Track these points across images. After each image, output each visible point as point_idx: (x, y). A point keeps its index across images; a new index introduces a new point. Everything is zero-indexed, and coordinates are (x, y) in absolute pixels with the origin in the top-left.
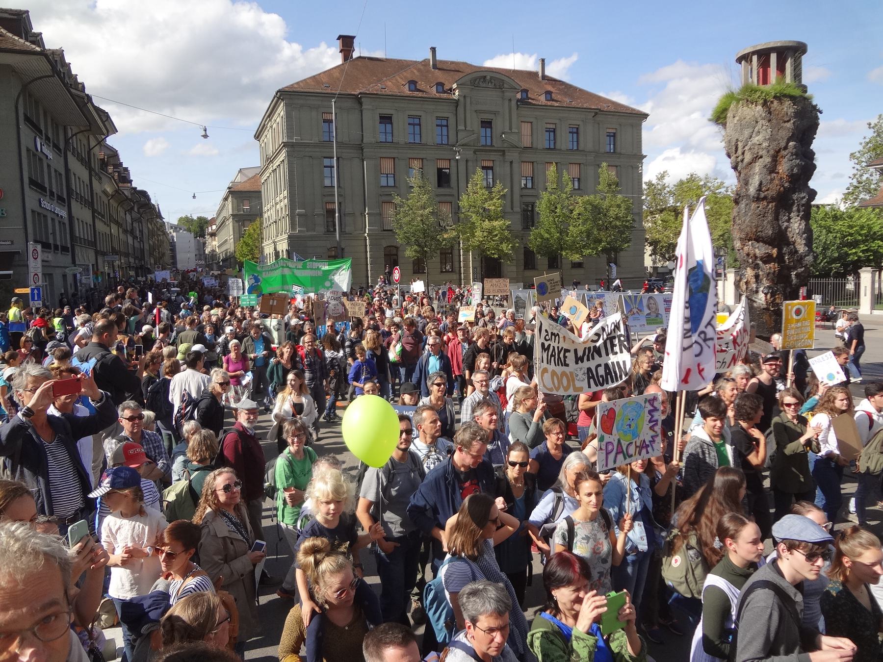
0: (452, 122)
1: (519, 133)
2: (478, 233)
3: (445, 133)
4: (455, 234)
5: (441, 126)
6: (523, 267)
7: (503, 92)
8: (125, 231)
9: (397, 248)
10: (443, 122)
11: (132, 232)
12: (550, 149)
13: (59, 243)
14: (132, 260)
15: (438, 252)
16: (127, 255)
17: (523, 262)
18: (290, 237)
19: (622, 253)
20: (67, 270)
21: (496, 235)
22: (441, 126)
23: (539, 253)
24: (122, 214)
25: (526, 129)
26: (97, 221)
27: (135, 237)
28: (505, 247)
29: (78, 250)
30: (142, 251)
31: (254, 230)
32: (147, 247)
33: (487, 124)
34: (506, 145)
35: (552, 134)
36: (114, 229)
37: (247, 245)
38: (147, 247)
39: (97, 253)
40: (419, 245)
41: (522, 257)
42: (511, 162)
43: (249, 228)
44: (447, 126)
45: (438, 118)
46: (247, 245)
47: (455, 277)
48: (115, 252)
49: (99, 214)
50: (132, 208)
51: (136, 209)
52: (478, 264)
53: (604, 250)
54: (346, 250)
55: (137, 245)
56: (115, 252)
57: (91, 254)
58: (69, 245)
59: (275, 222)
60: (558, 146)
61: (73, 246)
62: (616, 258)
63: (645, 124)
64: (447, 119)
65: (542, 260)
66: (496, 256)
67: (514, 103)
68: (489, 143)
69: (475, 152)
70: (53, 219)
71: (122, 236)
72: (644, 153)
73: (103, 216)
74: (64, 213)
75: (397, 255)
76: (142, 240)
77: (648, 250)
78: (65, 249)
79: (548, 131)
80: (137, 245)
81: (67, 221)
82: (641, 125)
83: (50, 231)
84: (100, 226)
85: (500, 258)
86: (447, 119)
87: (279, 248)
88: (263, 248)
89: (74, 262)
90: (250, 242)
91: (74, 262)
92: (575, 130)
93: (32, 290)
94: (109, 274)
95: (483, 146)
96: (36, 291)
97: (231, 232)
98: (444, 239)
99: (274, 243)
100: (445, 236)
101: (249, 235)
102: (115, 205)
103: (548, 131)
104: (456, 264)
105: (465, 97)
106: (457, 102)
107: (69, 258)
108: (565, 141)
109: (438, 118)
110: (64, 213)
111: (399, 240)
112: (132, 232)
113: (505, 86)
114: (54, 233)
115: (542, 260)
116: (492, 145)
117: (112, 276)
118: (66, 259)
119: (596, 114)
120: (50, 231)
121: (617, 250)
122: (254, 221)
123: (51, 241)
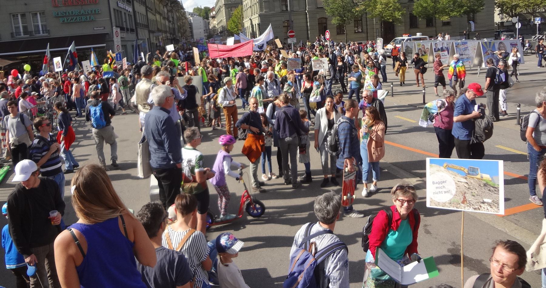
2: (379, 6)
4: (364, 7)
6: (409, 27)
8: (164, 18)
9: (326, 19)
11: (168, 19)
13: (129, 27)
14: (168, 35)
15: (353, 20)
16: (166, 32)
17: (408, 23)
18: (260, 16)
19: (478, 14)
21: (391, 7)
23: (420, 17)
24: (162, 8)
26: (148, 13)
27: (169, 22)
28: (398, 15)
29: (139, 30)
30: (174, 29)
36: (158, 16)
37: (234, 22)
39: (150, 32)
40: (340, 16)
41: (408, 20)
43: (235, 12)
46: (234, 22)
47: (364, 35)
48: (159, 31)
49: (149, 8)
50: (167, 4)
51: (169, 5)
52: (378, 26)
53: (465, 13)
55: (171, 26)
56: (159, 31)
57: (146, 32)
58: (134, 28)
59: (251, 7)
61: (136, 28)
62: (474, 17)
65: (422, 22)
66: (391, 20)
70: (125, 13)
71: (163, 21)
73: (152, 10)
74: (130, 9)
75: (326, 23)
77: (497, 11)
78: (132, 30)
80: (171, 26)
81: (132, 14)
83: (124, 20)
85: (393, 22)
87: (254, 24)
88: (243, 23)
90: (236, 20)
93: (117, 55)
96: (118, 55)
98: (357, 11)
99: (251, 19)
100: (357, 9)
102: (158, 3)
104: (365, 27)
110: (130, 9)
111: (328, 14)
112: (168, 19)
114: (126, 21)
115: (422, 22)
117: (158, 45)
118: (132, 36)
120: (124, 20)
121: (474, 11)
122: (238, 7)
123: (125, 26)
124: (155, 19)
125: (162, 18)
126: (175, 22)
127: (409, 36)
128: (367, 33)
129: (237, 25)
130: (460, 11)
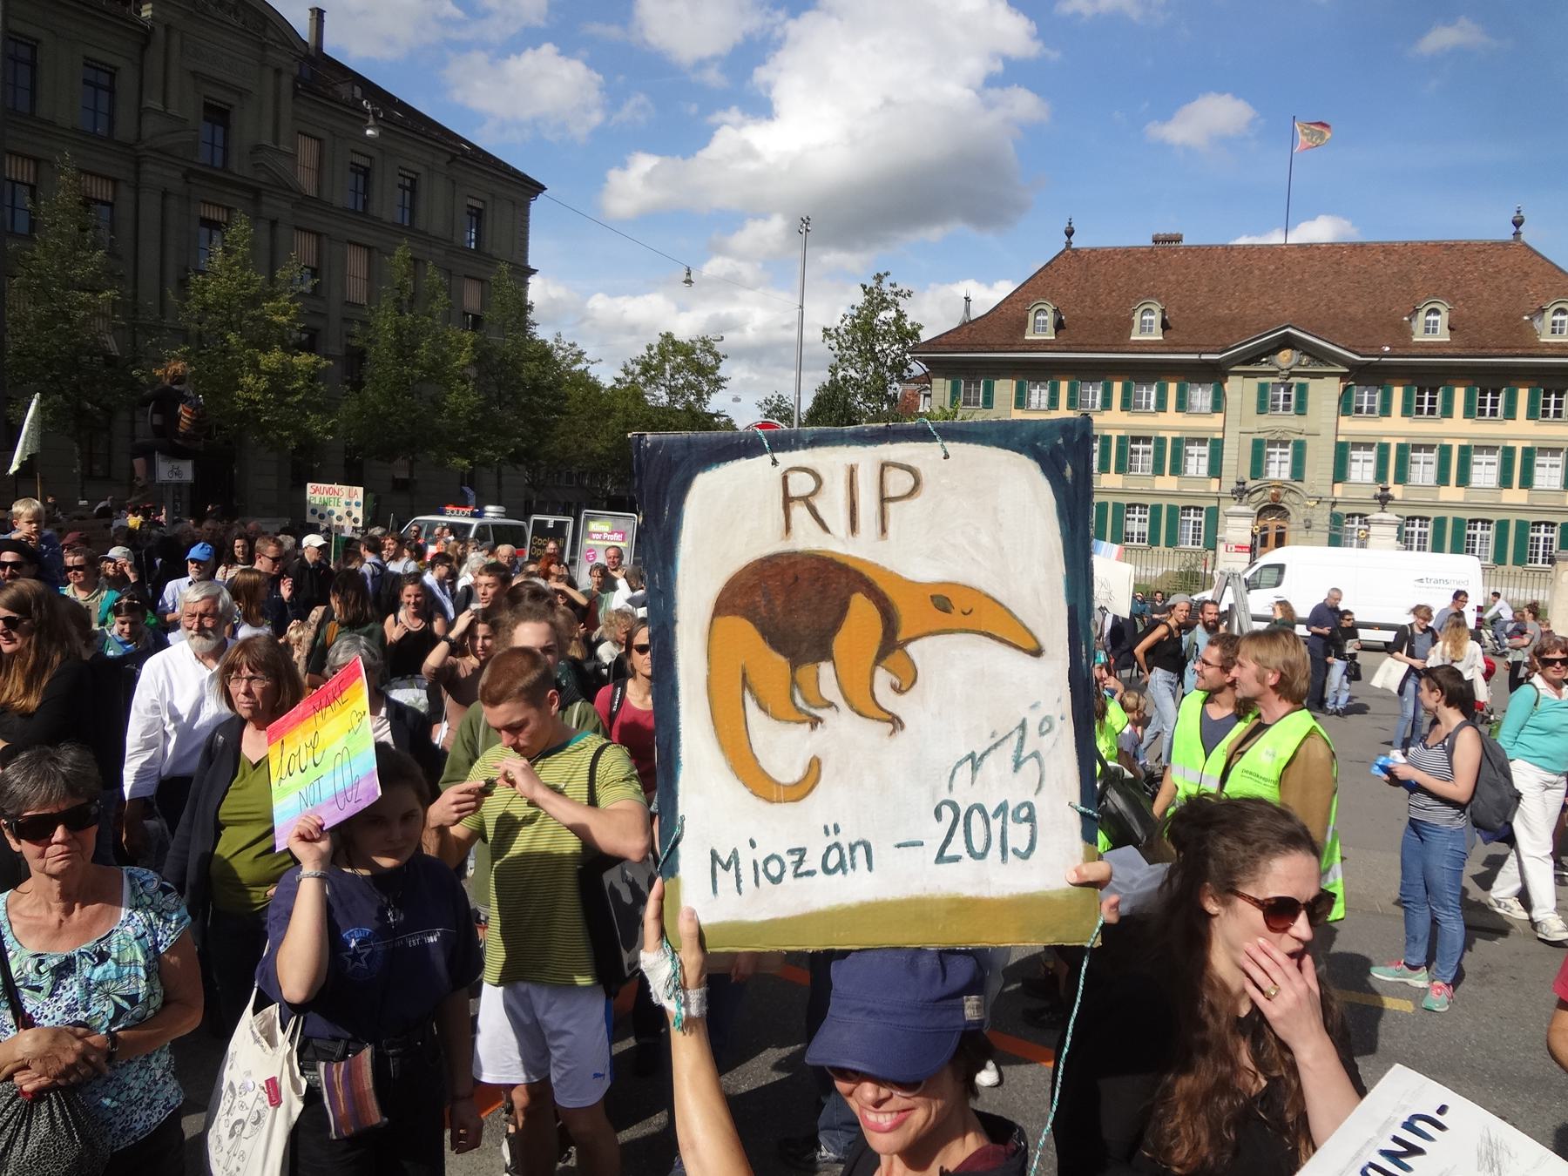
0: (127, 81)
1: (293, 156)
3: (103, 104)
5: (97, 87)
7: (263, 46)
10: (102, 80)
12: (355, 212)
22: (97, 87)
25: (307, 151)
33: (218, 115)
34: (263, 177)
35: (361, 178)
42: (274, 223)
44: (112, 91)
45: (89, 63)
60: (375, 209)
63: (537, 207)
64: (112, 73)
67: (286, 81)
68: (218, 164)
69: (185, 177)
72: (532, 263)
79: (355, 168)
82: (528, 205)
86: (112, 73)
92: (408, 183)
95: (205, 165)
103: (355, 168)
105: (168, 28)
106: (145, 36)
108: (388, 203)
109: (89, 63)
113: (271, 34)
116: (225, 168)
119: (454, 158)
130: (504, 449)
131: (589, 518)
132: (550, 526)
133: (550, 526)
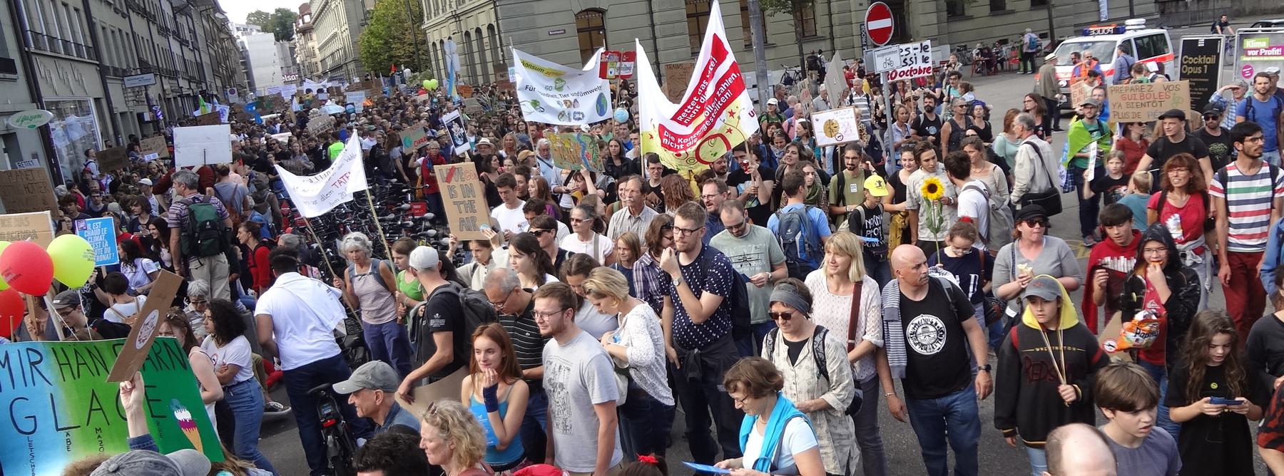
6: (945, 14)
8: (164, 31)
16: (173, 75)
20: (12, 122)
27: (183, 43)
30: (200, 66)
31: (387, 8)
32: (206, 59)
36: (140, 25)
38: (206, 59)
39: (103, 72)
46: (378, 37)
54: (608, 15)
55: (189, 55)
57: (91, 78)
71: (158, 39)
76: (195, 48)
80: (189, 55)
84: (101, 14)
89: (36, 97)
91: (36, 97)
94: (140, 116)
97: (343, 18)
99: (456, 17)
101: (378, 20)
104: (822, 22)
107: (20, 88)
112: (177, 35)
117: (147, 117)
124: (125, 27)
125: (154, 29)
126: (201, 44)
127: (1148, 24)
128: (832, 38)
129: (386, 43)
131: (1243, 37)
132: (1201, 44)
133: (1201, 44)
